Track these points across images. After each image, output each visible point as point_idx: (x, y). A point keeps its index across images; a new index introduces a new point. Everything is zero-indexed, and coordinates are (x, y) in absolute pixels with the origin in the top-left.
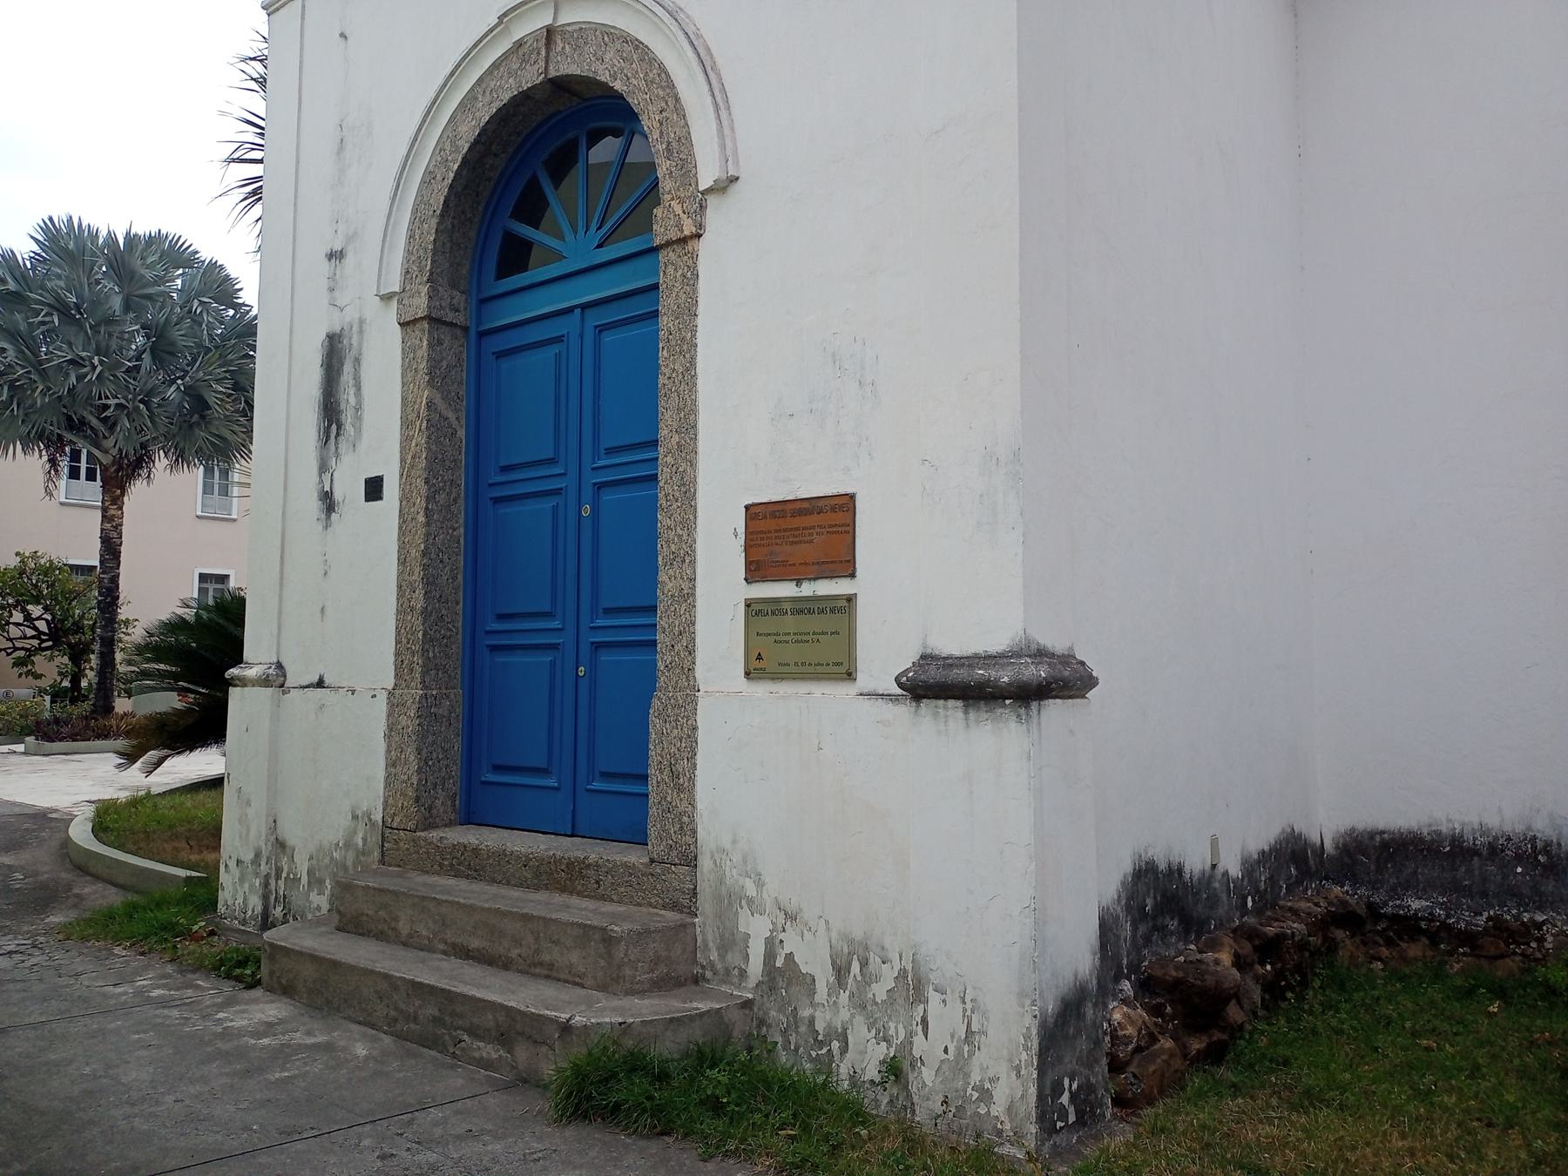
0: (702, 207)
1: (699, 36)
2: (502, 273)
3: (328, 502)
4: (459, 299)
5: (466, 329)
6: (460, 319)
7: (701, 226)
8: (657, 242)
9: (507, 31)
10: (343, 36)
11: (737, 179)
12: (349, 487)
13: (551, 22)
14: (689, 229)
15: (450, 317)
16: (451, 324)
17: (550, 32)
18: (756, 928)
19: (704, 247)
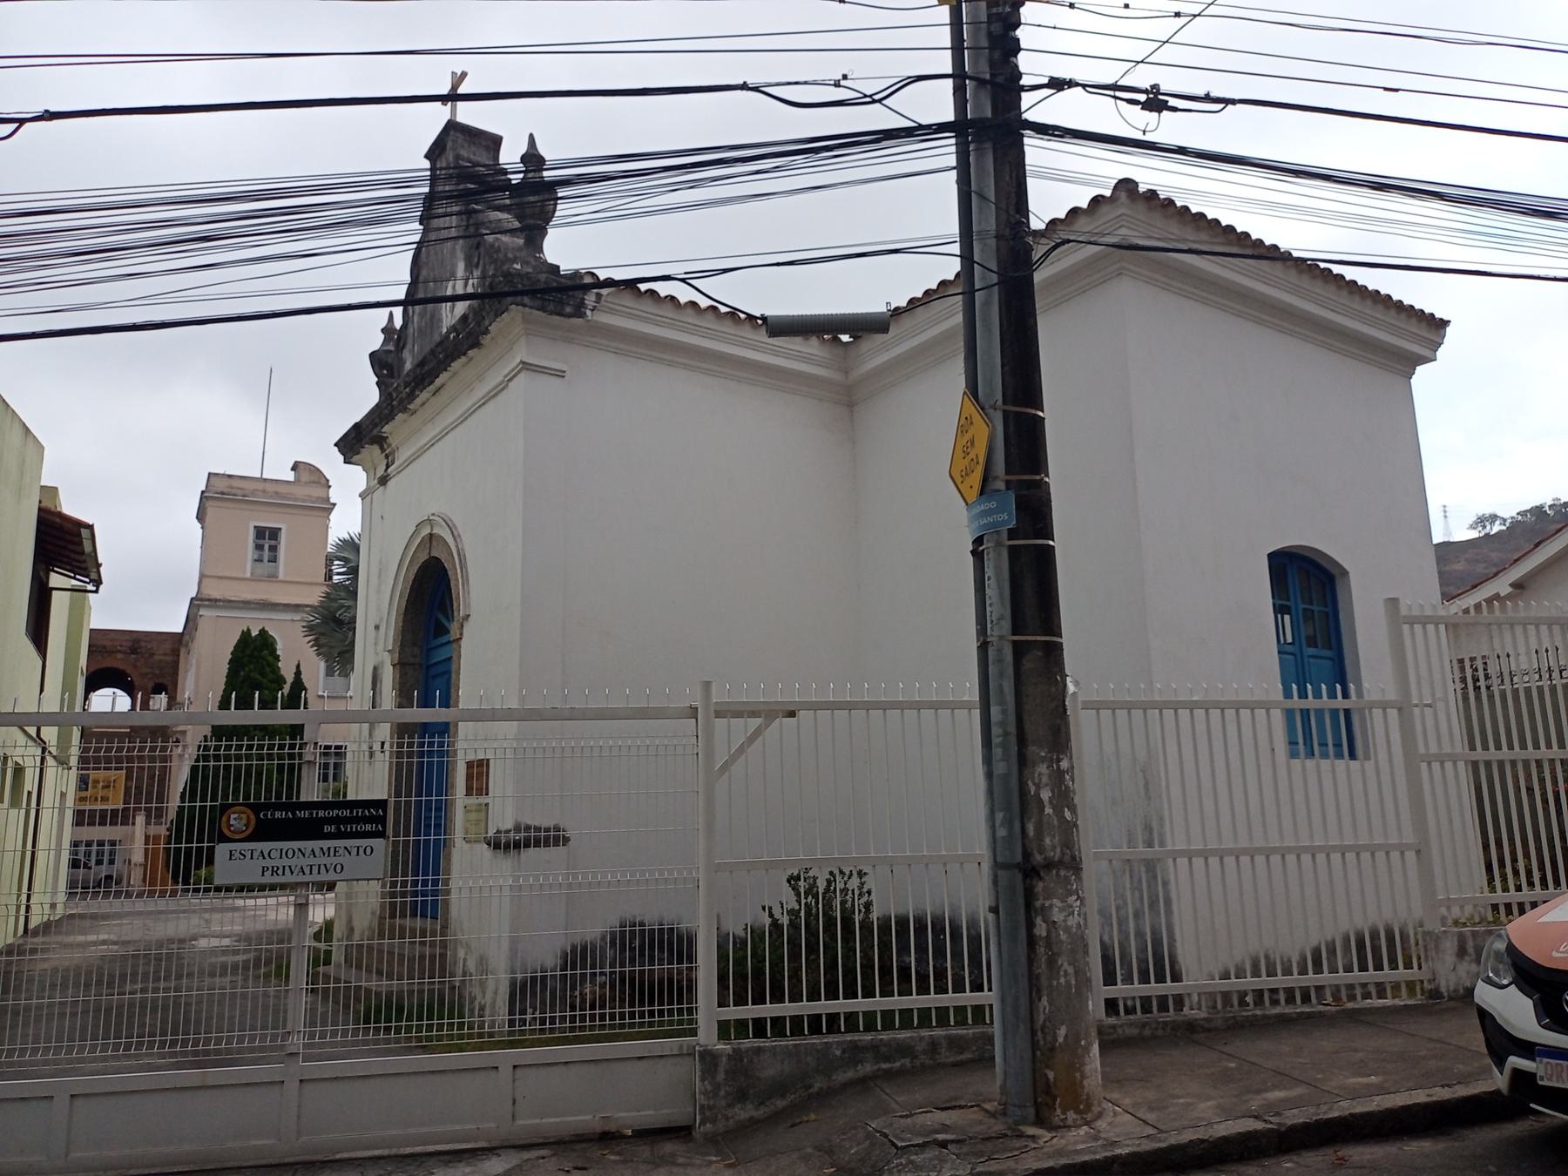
0: (462, 626)
1: (463, 550)
2: (435, 637)
3: (371, 755)
4: (416, 650)
5: (421, 665)
6: (418, 660)
7: (461, 634)
8: (452, 640)
9: (419, 533)
10: (382, 517)
11: (469, 615)
12: (377, 747)
13: (429, 532)
14: (458, 636)
15: (412, 660)
16: (412, 664)
17: (431, 534)
18: (461, 953)
19: (464, 643)
